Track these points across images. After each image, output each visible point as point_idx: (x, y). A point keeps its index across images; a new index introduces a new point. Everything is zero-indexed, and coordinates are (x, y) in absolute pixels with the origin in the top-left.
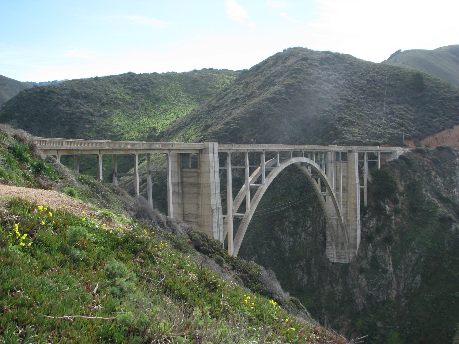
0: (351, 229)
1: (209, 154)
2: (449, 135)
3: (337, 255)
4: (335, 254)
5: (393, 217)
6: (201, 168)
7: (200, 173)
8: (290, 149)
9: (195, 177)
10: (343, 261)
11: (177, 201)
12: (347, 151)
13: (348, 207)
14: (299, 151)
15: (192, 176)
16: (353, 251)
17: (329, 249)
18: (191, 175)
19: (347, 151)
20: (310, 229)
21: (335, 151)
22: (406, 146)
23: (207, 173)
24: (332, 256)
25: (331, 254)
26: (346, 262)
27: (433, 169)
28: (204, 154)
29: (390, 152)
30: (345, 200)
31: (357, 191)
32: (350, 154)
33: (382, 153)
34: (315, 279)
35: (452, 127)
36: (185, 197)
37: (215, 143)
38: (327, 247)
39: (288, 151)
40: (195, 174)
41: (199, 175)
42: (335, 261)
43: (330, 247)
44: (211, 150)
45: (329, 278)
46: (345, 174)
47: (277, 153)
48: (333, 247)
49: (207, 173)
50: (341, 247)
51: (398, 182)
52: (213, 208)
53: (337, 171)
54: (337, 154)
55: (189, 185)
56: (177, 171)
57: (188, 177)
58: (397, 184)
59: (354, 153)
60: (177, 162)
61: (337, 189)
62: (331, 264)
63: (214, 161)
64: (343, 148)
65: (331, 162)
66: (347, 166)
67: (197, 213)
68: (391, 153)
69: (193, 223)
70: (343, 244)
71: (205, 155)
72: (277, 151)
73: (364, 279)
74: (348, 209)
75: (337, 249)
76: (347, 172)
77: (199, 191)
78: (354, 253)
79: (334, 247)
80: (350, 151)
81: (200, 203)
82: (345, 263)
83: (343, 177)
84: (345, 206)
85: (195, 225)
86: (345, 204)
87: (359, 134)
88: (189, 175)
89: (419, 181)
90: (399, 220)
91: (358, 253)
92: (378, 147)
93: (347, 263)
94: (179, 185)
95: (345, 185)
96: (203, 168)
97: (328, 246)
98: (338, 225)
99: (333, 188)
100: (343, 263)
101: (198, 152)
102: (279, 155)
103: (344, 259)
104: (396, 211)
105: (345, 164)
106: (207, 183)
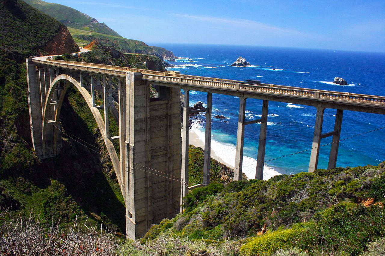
4: (44, 152)
7: (172, 104)
10: (51, 156)
11: (144, 139)
15: (160, 109)
16: (58, 146)
20: (11, 136)
23: (177, 103)
24: (41, 154)
25: (40, 153)
26: (54, 156)
49: (177, 103)
52: (181, 136)
60: (144, 96)
67: (165, 145)
69: (160, 156)
73: (78, 164)
82: (53, 156)
85: (162, 158)
91: (63, 145)
93: (55, 156)
103: (52, 154)
106: (178, 114)
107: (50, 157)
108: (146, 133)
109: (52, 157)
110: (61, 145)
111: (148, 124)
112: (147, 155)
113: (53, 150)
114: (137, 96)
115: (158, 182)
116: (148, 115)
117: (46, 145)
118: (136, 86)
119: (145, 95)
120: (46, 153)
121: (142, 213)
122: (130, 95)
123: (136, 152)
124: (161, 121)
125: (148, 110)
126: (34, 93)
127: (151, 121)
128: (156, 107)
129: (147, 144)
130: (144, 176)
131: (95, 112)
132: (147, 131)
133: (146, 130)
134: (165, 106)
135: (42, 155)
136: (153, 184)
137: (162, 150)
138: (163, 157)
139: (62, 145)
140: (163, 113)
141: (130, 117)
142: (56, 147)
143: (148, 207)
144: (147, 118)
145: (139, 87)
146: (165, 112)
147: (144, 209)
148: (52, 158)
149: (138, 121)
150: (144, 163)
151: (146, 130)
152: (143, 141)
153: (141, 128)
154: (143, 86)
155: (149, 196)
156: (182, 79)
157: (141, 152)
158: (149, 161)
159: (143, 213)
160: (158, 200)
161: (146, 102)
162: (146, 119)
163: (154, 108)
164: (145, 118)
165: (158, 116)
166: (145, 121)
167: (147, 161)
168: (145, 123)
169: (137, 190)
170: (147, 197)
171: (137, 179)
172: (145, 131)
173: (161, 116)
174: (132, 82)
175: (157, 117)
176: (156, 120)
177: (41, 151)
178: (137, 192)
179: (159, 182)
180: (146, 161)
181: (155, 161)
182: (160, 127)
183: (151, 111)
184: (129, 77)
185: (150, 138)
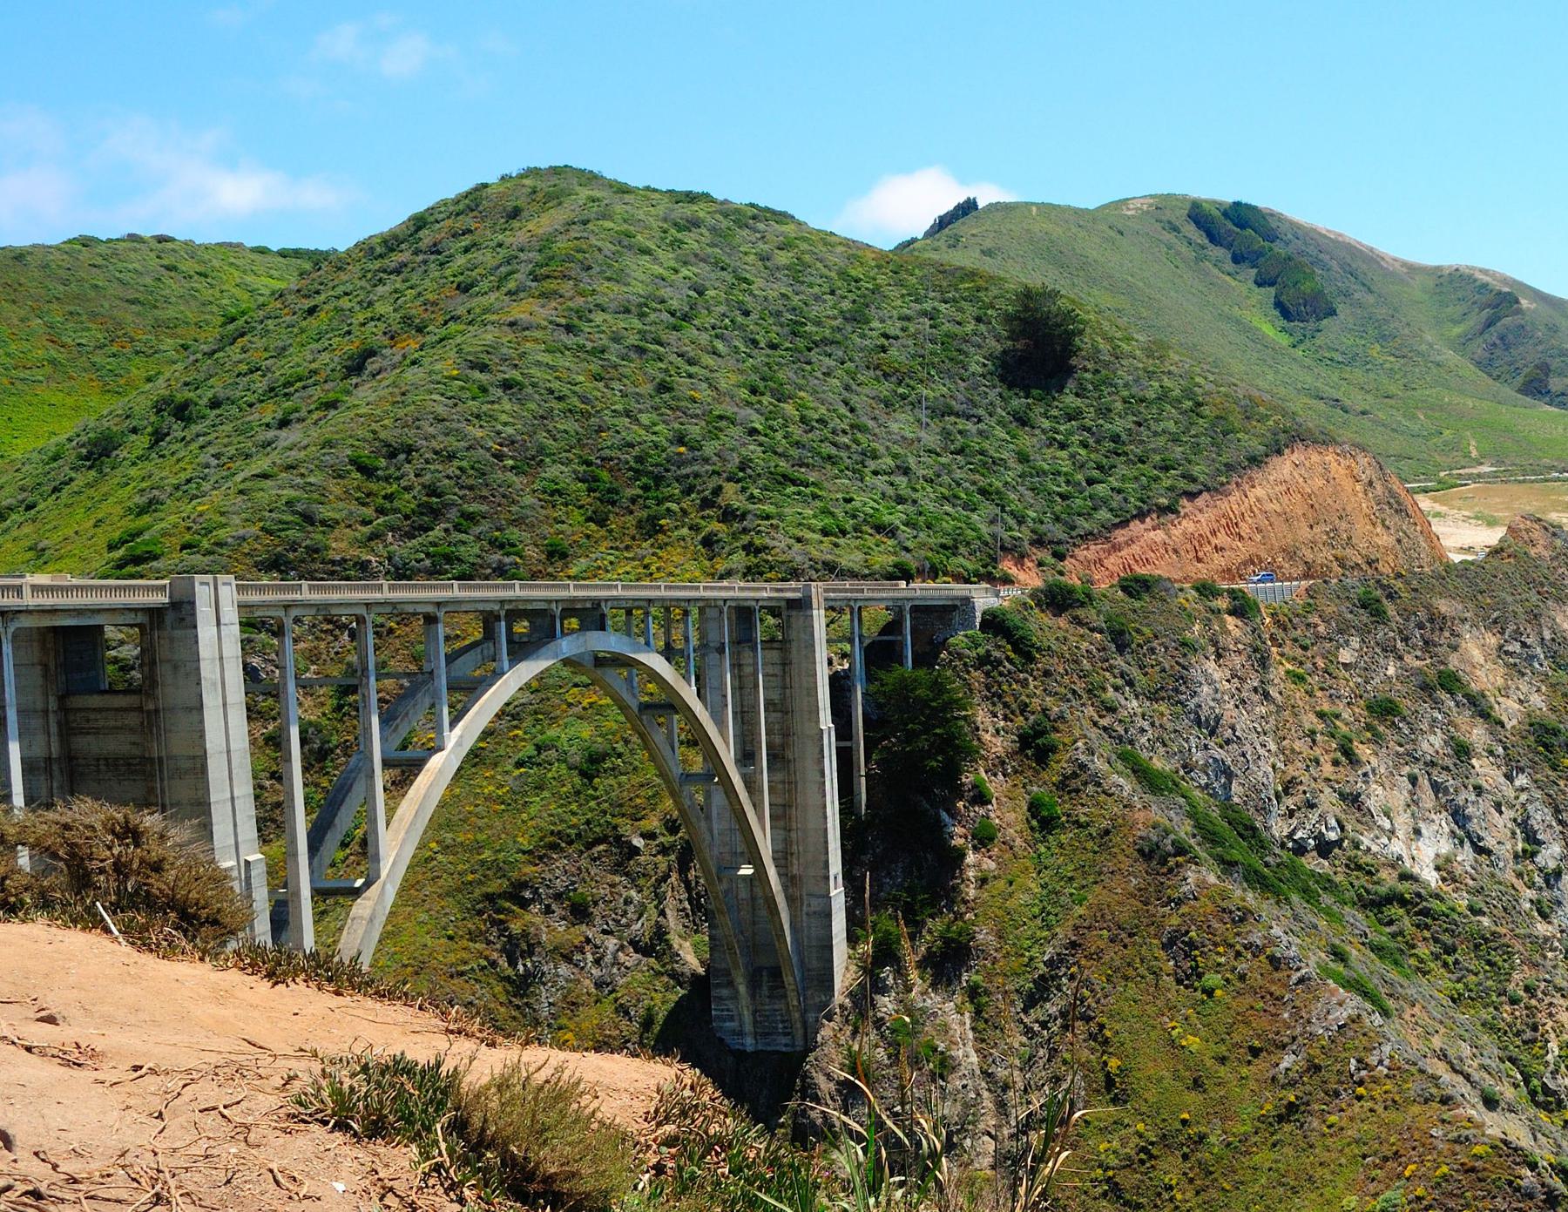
0: (807, 914)
1: (195, 627)
2: (1165, 537)
3: (755, 1022)
6: (159, 691)
7: (157, 711)
8: (550, 601)
9: (132, 730)
10: (781, 1043)
12: (783, 604)
14: (588, 605)
17: (721, 998)
19: (783, 604)
21: (734, 604)
22: (1007, 580)
25: (731, 1019)
26: (793, 1045)
27: (1110, 669)
28: (172, 628)
29: (950, 603)
30: (780, 801)
31: (826, 761)
32: (794, 613)
33: (915, 609)
35: (1171, 509)
37: (221, 578)
38: (713, 993)
39: (543, 606)
40: (133, 719)
41: (151, 721)
42: (749, 1043)
43: (725, 992)
44: (204, 611)
46: (776, 696)
47: (498, 618)
48: (737, 992)
50: (771, 988)
51: (982, 716)
53: (744, 687)
54: (744, 614)
58: (977, 729)
59: (809, 613)
61: (746, 756)
62: (730, 1059)
63: (221, 658)
64: (765, 591)
65: (721, 650)
66: (784, 664)
68: (955, 607)
70: (776, 973)
71: (178, 633)
72: (496, 607)
74: (793, 835)
75: (753, 996)
76: (784, 688)
77: (151, 790)
79: (742, 989)
80: (793, 604)
82: (789, 1049)
83: (769, 704)
84: (782, 823)
86: (782, 816)
87: (825, 532)
89: (1061, 717)
92: (903, 584)
93: (798, 1049)
95: (778, 740)
96: (171, 693)
97: (718, 986)
98: (753, 899)
99: (728, 756)
100: (778, 1052)
101: (140, 619)
102: (503, 623)
104: (983, 839)
105: (775, 655)
109: (784, 1049)
135: (741, 1034)
140: (128, 747)
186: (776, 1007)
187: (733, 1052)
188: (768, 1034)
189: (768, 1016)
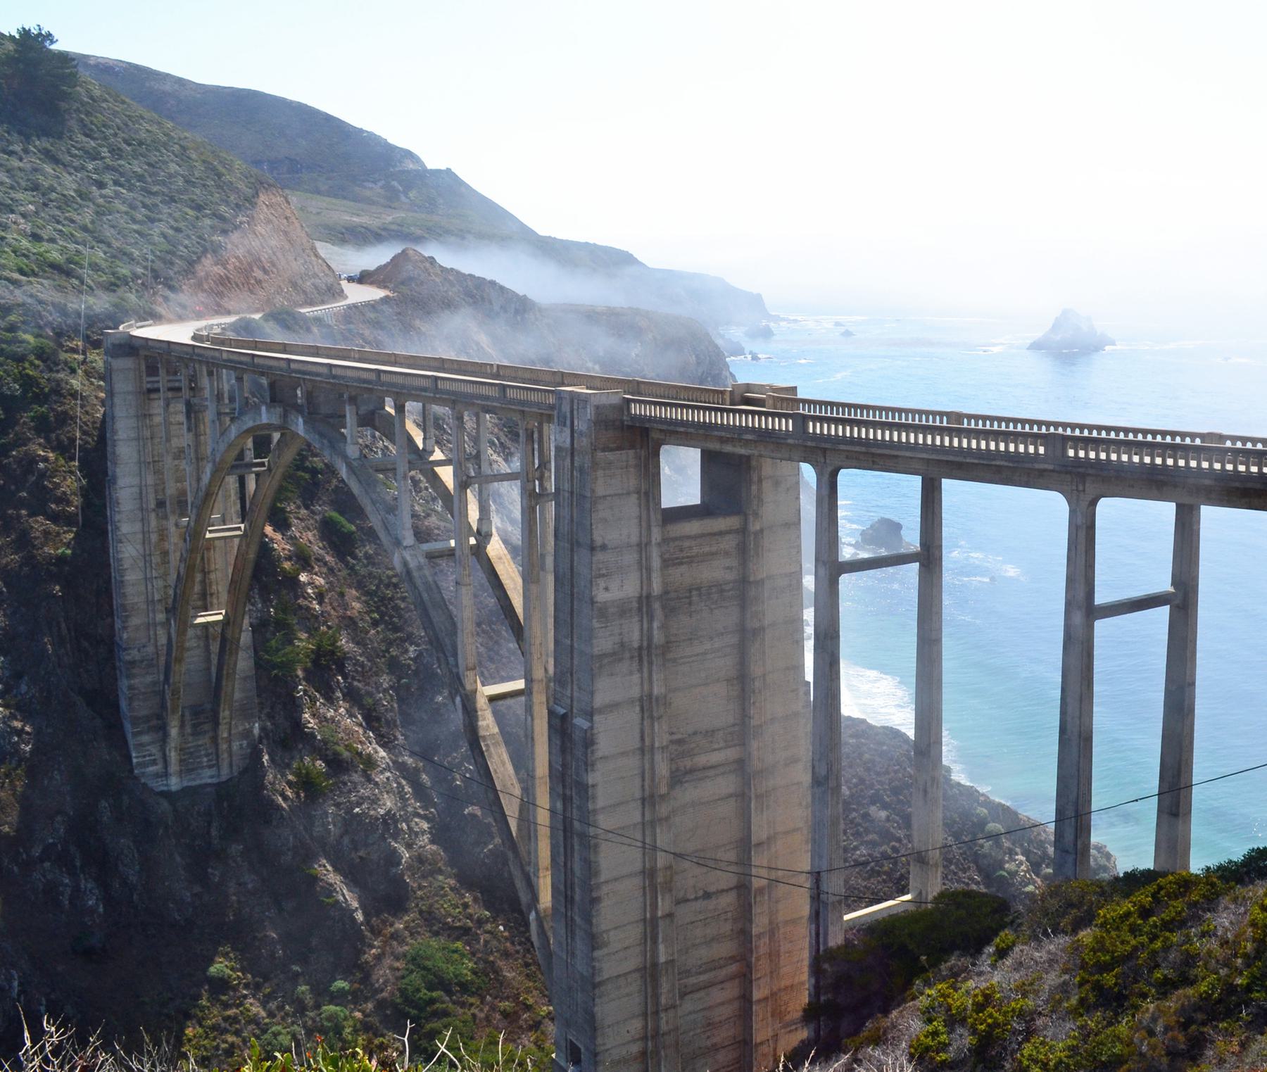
4: (173, 756)
5: (303, 577)
7: (762, 531)
9: (727, 554)
10: (206, 777)
11: (635, 692)
13: (213, 567)
15: (713, 554)
16: (241, 728)
17: (141, 745)
18: (707, 549)
20: (24, 688)
23: (787, 525)
24: (157, 768)
25: (154, 762)
26: (219, 776)
34: (133, 879)
36: (674, 660)
42: (174, 783)
45: (178, 859)
49: (787, 525)
50: (194, 726)
55: (695, 599)
56: (634, 539)
57: (691, 560)
69: (712, 773)
78: (247, 734)
81: (756, 670)
82: (215, 780)
88: (695, 550)
90: (322, 581)
91: (262, 729)
93: (224, 778)
94: (657, 606)
97: (140, 733)
103: (210, 767)
107: (203, 781)
108: (645, 664)
109: (209, 781)
110: (252, 727)
111: (656, 625)
112: (652, 768)
113: (217, 749)
114: (605, 497)
115: (701, 893)
116: (657, 588)
117: (182, 726)
118: (600, 455)
119: (638, 493)
120: (181, 761)
121: (629, 1042)
122: (572, 493)
123: (599, 754)
124: (712, 610)
125: (656, 563)
126: (136, 490)
127: (670, 611)
128: (690, 548)
129: (651, 717)
130: (638, 866)
131: (415, 574)
132: (649, 655)
133: (645, 653)
134: (729, 543)
135: (166, 775)
136: (678, 902)
137: (722, 744)
138: (723, 774)
139: (257, 725)
141: (572, 595)
142: (230, 734)
143: (656, 1013)
144: (648, 597)
145: (610, 456)
146: (728, 568)
147: (636, 1025)
148: (210, 785)
149: (611, 610)
150: (639, 802)
151: (645, 653)
152: (631, 701)
153: (622, 644)
154: (631, 452)
155: (662, 959)
156: (805, 419)
157: (622, 754)
158: (662, 797)
159: (634, 1041)
160: (702, 978)
161: (644, 524)
162: (645, 601)
163: (681, 550)
164: (640, 598)
165: (699, 589)
166: (640, 609)
167: (652, 796)
168: (641, 621)
169: (607, 931)
170: (655, 965)
171: (607, 882)
172: (641, 660)
173: (714, 590)
174: (581, 434)
175: (694, 593)
176: (690, 604)
177: (158, 756)
178: (606, 944)
179: (707, 895)
180: (647, 793)
181: (689, 793)
182: (711, 638)
183: (667, 563)
184: (568, 415)
185: (663, 690)
186: (200, 743)
187: (162, 794)
188: (193, 770)
189: (191, 753)
